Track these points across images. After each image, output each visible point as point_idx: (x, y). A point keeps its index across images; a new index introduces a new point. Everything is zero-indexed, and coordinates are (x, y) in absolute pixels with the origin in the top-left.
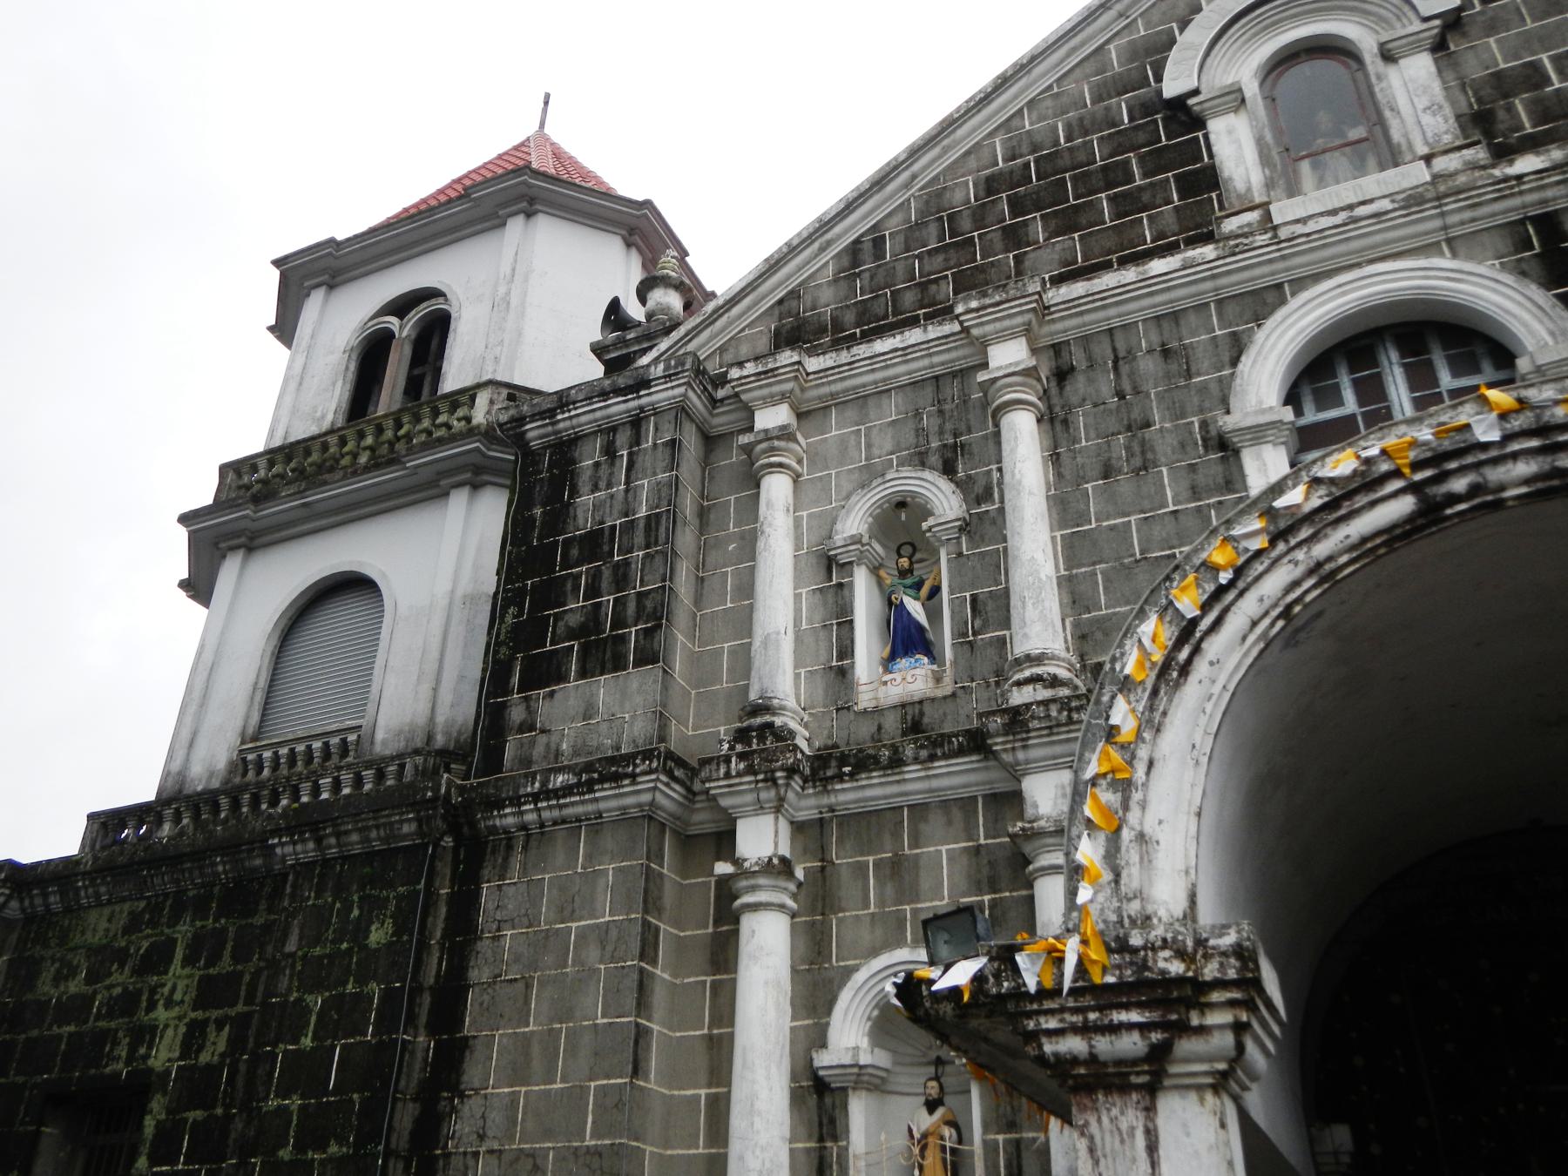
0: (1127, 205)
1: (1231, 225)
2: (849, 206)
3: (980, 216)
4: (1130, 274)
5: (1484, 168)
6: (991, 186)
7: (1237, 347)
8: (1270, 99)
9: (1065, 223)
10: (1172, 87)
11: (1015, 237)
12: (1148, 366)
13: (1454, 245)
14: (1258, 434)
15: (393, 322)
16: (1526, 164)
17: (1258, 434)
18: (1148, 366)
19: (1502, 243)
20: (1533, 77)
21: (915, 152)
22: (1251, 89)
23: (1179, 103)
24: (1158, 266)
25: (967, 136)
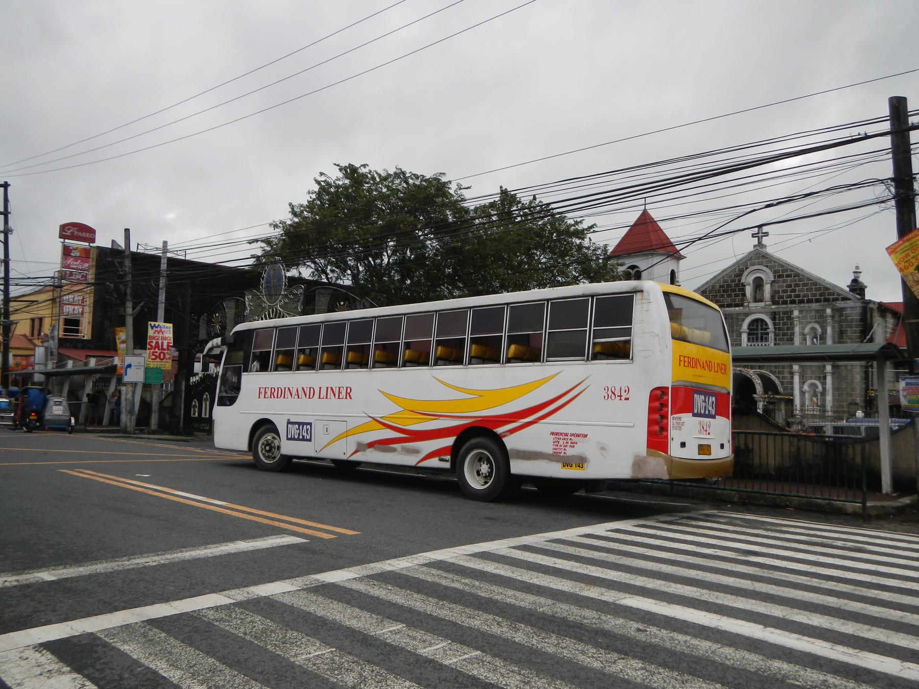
0: (736, 295)
1: (745, 304)
2: (703, 286)
3: (719, 291)
4: (733, 309)
5: (770, 305)
6: (720, 287)
7: (743, 320)
8: (753, 284)
9: (729, 296)
10: (743, 280)
11: (723, 296)
12: (735, 320)
13: (766, 313)
14: (744, 332)
15: (630, 270)
16: (773, 307)
17: (744, 332)
18: (735, 320)
19: (770, 314)
20: (779, 292)
21: (711, 280)
22: (751, 283)
23: (742, 284)
24: (737, 308)
25: (719, 277)
